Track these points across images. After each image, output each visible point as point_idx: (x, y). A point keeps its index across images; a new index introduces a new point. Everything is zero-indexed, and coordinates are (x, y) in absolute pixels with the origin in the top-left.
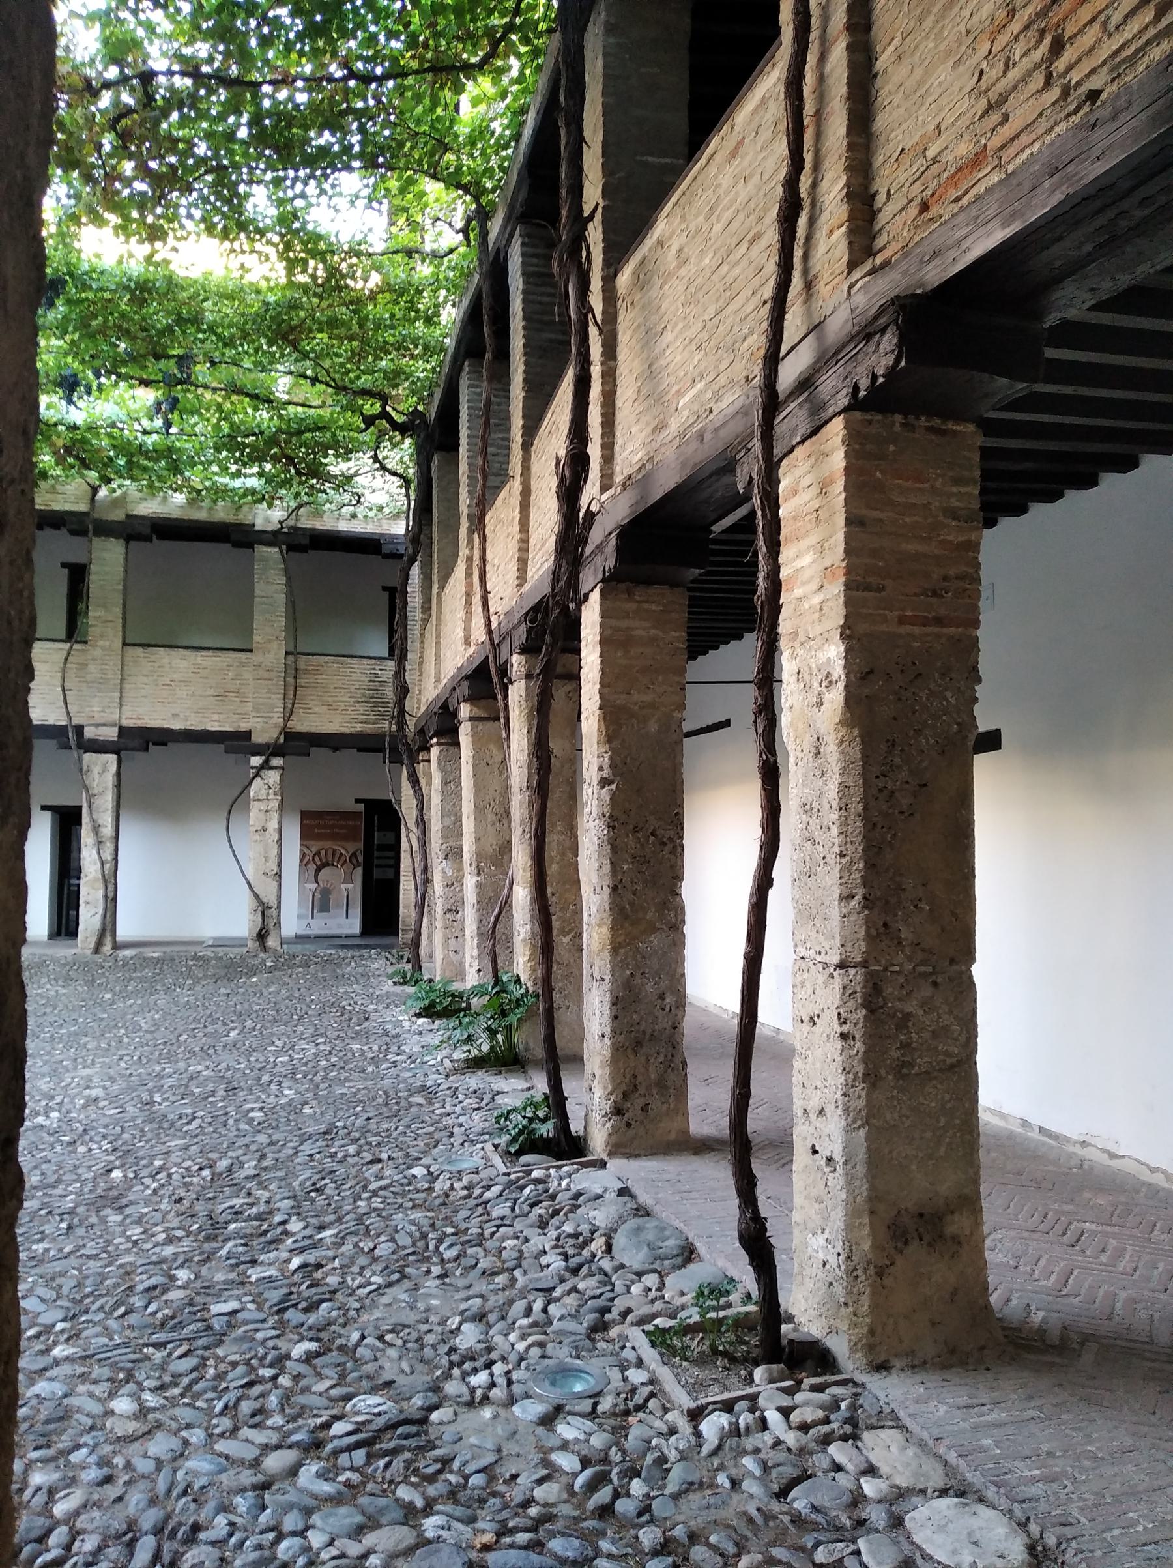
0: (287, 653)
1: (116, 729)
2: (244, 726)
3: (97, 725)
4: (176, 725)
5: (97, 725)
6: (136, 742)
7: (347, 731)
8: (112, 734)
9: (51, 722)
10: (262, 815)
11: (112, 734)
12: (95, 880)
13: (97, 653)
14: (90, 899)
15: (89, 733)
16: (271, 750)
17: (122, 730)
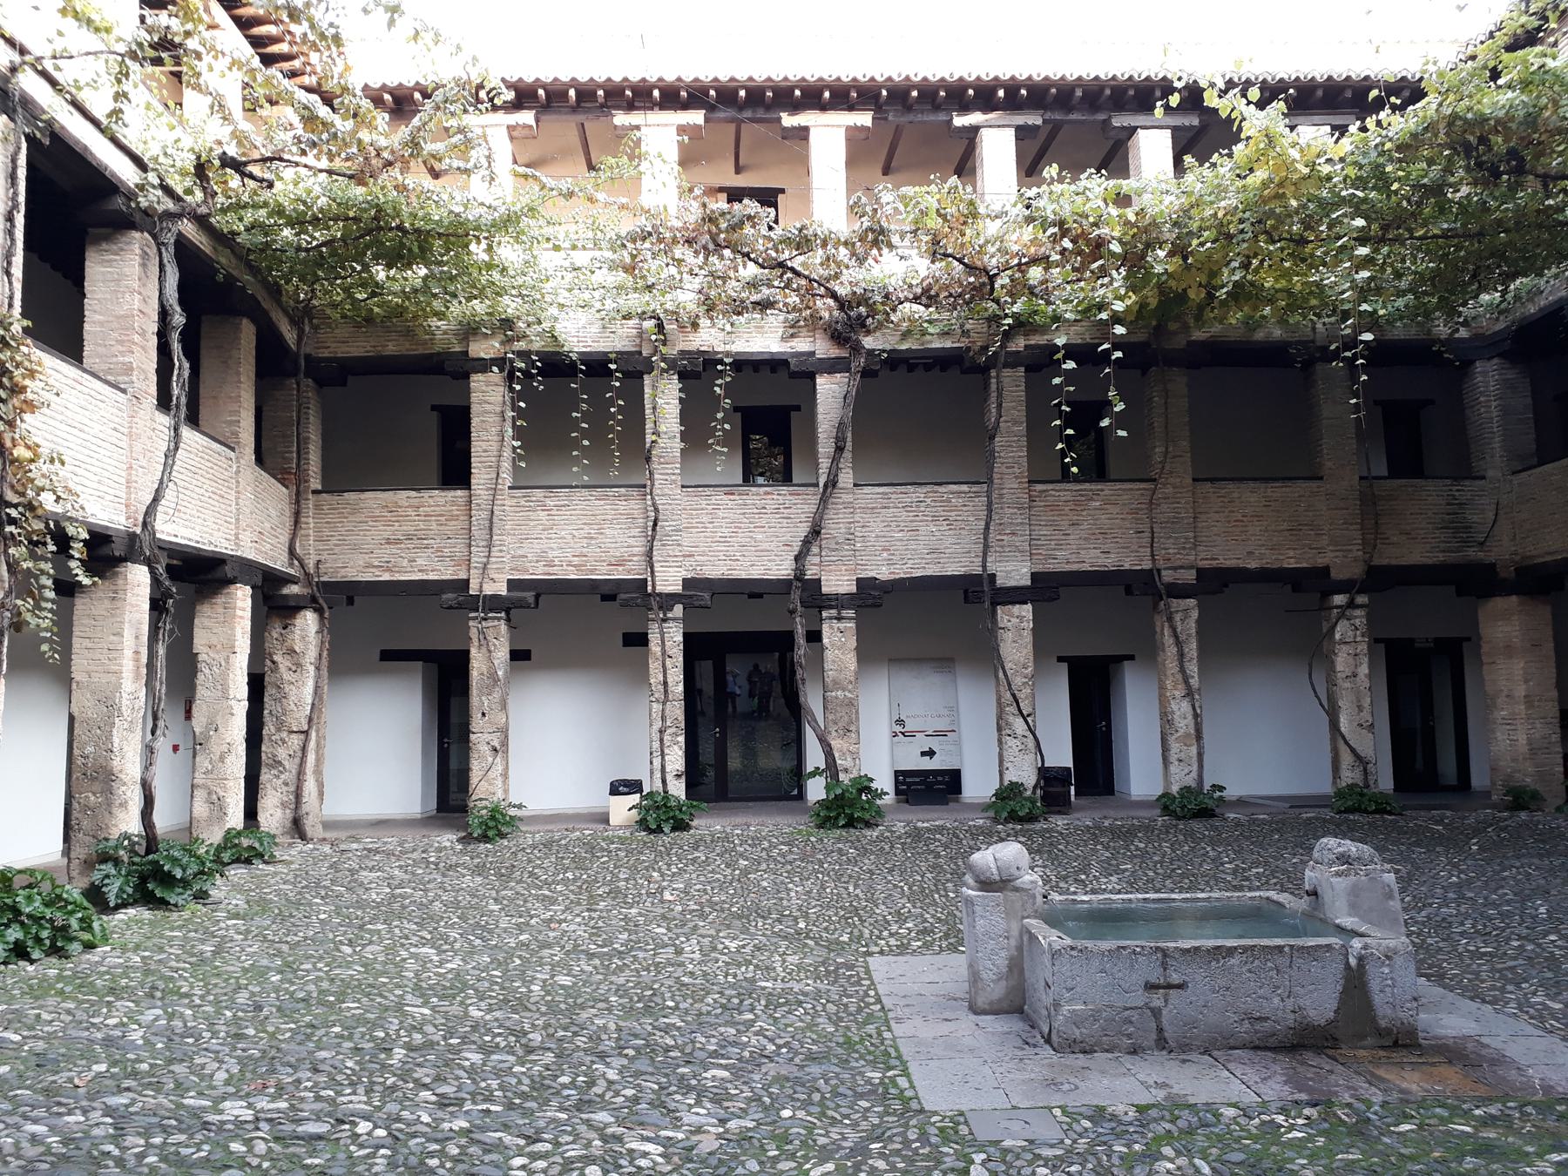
0: (1361, 478)
1: (1194, 572)
2: (1321, 561)
3: (1175, 569)
4: (1253, 565)
5: (1175, 569)
6: (1213, 584)
7: (1430, 562)
8: (1190, 576)
9: (1127, 566)
10: (1351, 660)
11: (1190, 576)
12: (1187, 735)
13: (1169, 490)
14: (1182, 756)
15: (1168, 577)
16: (1345, 587)
17: (1200, 571)
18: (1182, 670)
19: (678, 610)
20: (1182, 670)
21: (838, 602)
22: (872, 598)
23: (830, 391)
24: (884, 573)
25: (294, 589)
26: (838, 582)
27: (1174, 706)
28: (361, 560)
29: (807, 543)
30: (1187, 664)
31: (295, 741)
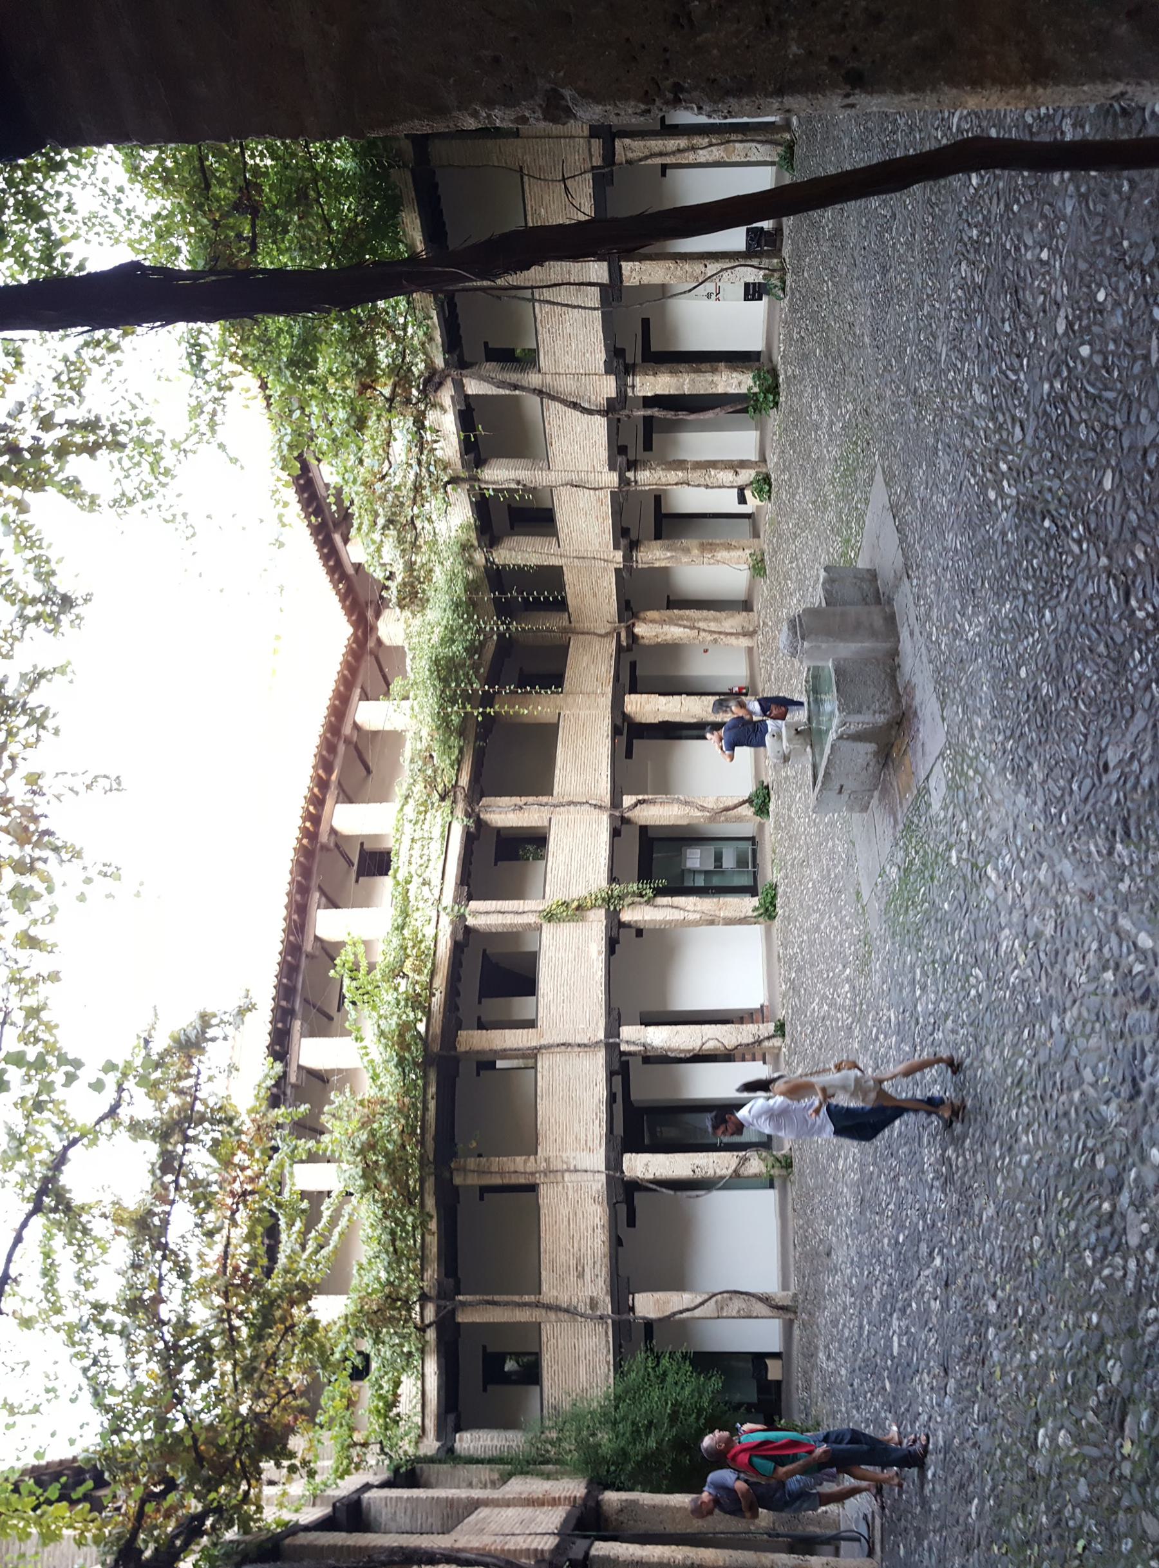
3: (591, 155)
5: (591, 155)
12: (725, 150)
15: (597, 161)
17: (592, 136)
18: (673, 153)
19: (630, 475)
20: (673, 153)
21: (622, 388)
22: (620, 362)
23: (473, 387)
24: (601, 356)
25: (623, 635)
26: (608, 387)
27: (703, 160)
28: (605, 607)
29: (585, 411)
30: (669, 149)
31: (703, 634)
